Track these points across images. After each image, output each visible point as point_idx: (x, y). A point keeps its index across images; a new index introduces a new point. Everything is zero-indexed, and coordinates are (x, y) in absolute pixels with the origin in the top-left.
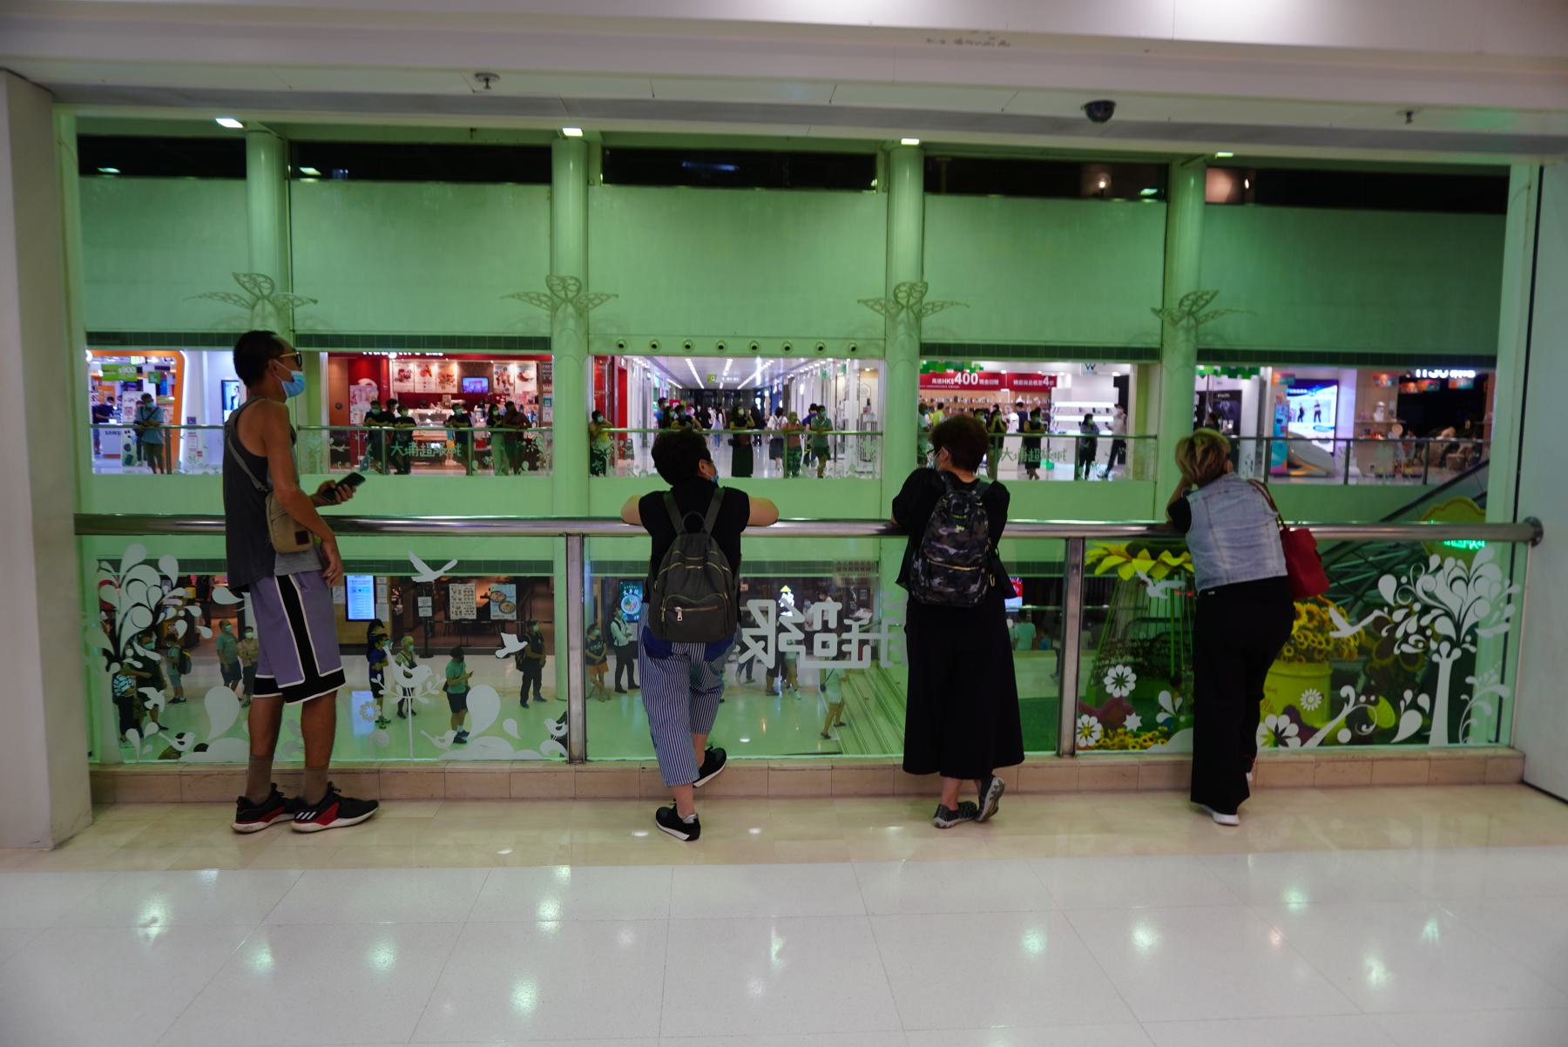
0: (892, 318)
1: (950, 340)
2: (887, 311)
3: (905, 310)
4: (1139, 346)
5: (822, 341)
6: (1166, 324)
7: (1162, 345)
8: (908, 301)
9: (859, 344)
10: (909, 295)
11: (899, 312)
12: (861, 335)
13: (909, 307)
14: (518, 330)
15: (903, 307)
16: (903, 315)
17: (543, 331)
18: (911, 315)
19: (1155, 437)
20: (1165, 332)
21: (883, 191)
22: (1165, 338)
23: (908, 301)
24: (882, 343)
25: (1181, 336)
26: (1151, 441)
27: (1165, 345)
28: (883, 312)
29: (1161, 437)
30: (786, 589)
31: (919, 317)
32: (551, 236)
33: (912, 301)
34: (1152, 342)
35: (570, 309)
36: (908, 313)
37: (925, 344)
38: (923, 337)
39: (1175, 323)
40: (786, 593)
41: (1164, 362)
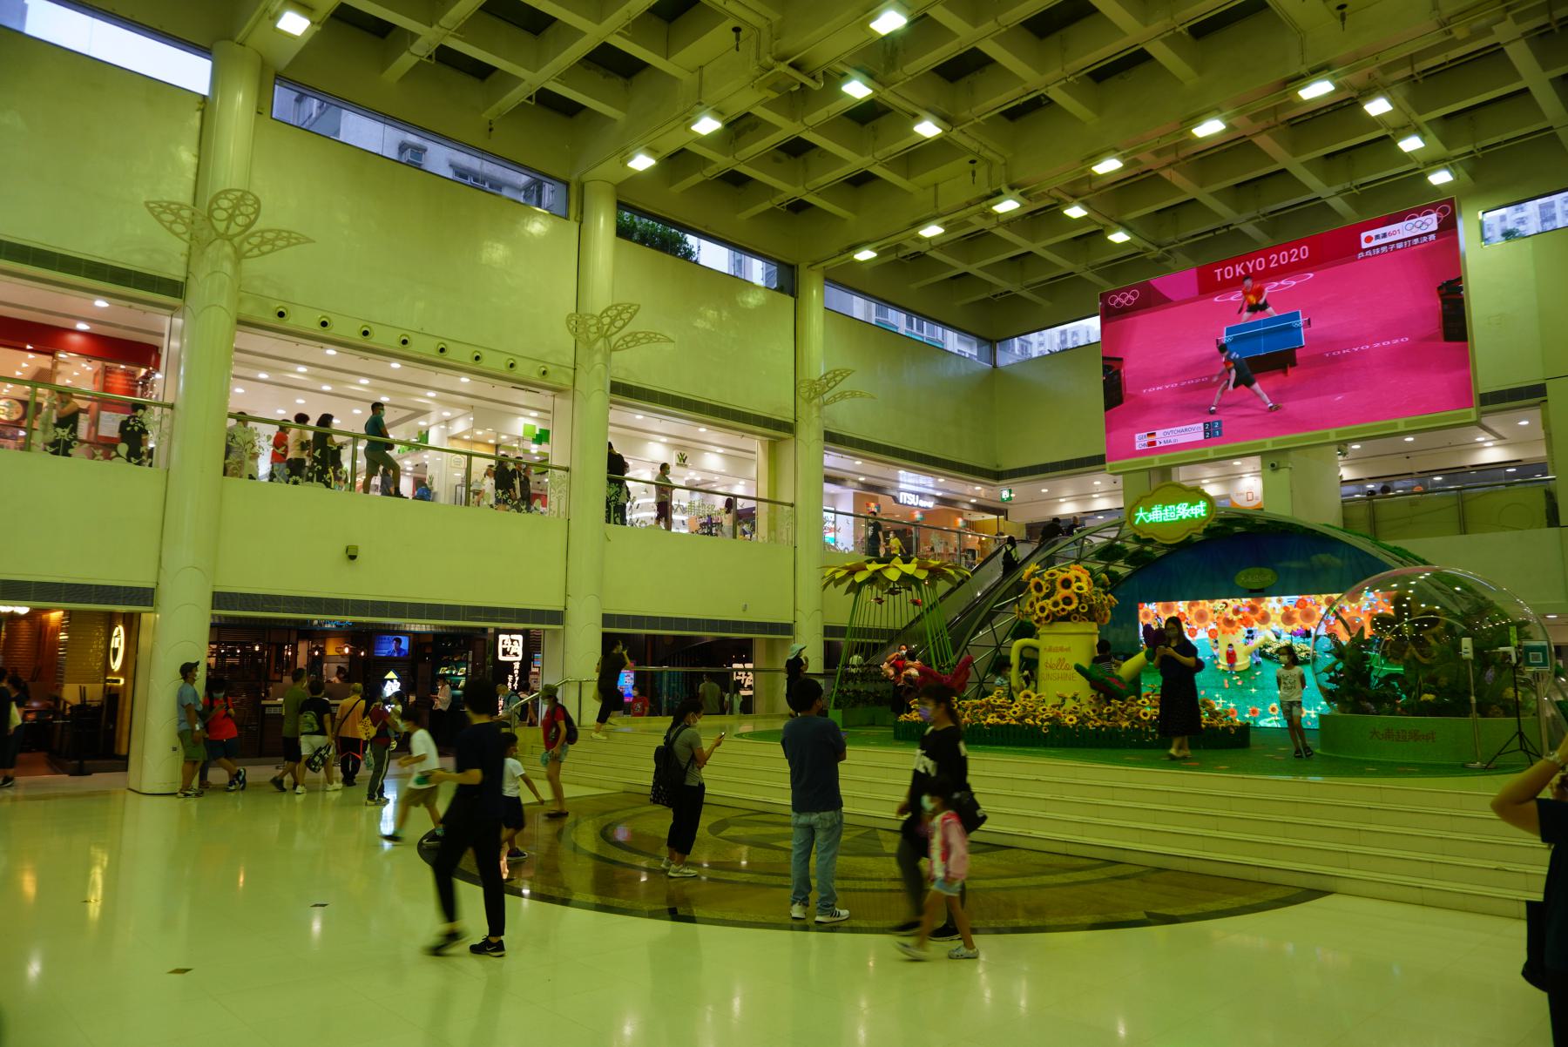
1: (632, 382)
4: (780, 418)
8: (608, 330)
9: (550, 368)
11: (596, 340)
12: (551, 359)
14: (135, 261)
16: (600, 344)
17: (175, 272)
19: (792, 505)
20: (798, 410)
23: (608, 330)
26: (787, 508)
27: (800, 420)
29: (799, 504)
30: (391, 675)
34: (788, 416)
35: (228, 249)
36: (605, 344)
40: (392, 680)
41: (799, 436)
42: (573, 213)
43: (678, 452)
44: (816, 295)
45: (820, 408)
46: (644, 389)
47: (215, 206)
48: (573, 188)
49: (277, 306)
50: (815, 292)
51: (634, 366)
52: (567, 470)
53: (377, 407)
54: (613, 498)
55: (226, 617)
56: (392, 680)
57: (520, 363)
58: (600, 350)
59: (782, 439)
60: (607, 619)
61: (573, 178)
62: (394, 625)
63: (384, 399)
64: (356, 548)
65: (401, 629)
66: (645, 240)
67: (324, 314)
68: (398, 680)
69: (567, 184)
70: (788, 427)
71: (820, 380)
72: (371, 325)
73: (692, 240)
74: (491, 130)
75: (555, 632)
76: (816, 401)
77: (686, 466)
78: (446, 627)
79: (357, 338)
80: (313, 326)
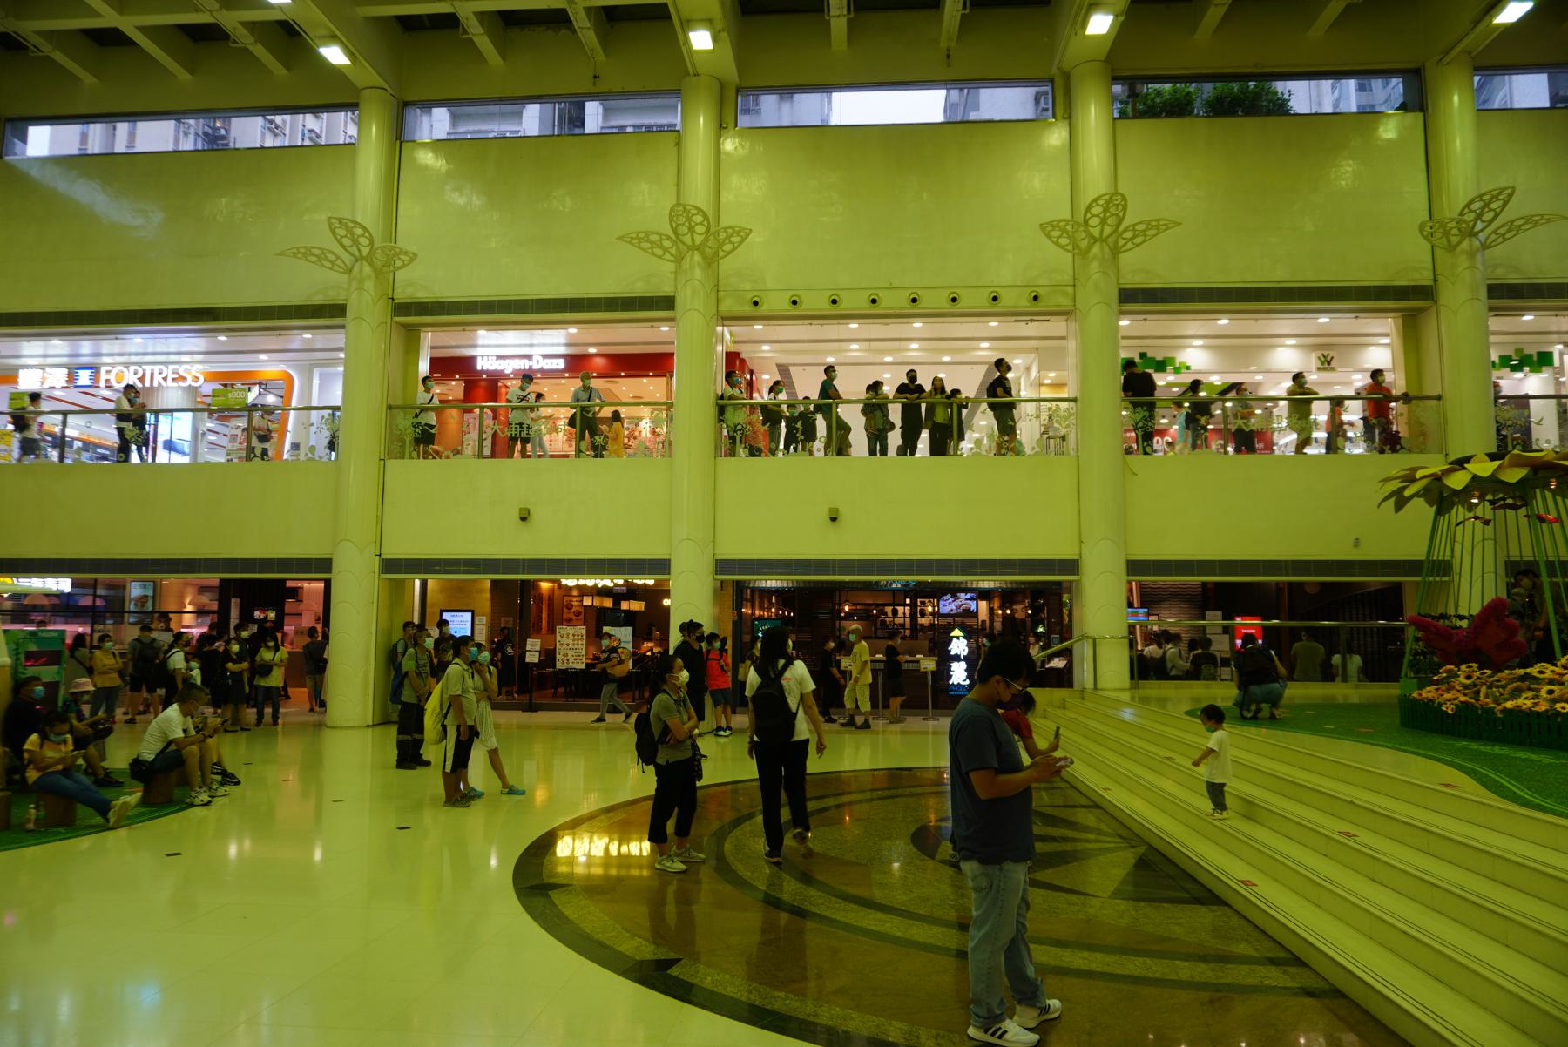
0: (1080, 254)
2: (1076, 246)
3: (1098, 244)
5: (996, 289)
6: (1439, 252)
7: (1435, 281)
8: (1102, 231)
9: (1041, 292)
10: (1103, 222)
11: (1090, 246)
12: (1043, 281)
13: (1103, 240)
14: (639, 289)
15: (1096, 241)
16: (1096, 249)
17: (666, 290)
18: (1107, 250)
19: (1439, 398)
21: (1064, 118)
22: (1439, 271)
23: (1102, 231)
24: (1070, 290)
25: (1463, 262)
27: (1440, 278)
28: (1070, 247)
29: (1447, 395)
30: (957, 632)
31: (1116, 252)
32: (678, 185)
33: (1107, 230)
34: (1423, 277)
35: (697, 257)
36: (1102, 248)
37: (1125, 289)
38: (1121, 281)
39: (1452, 248)
40: (958, 638)
42: (1059, 113)
43: (1319, 353)
44: (1456, 103)
45: (1471, 254)
46: (1174, 289)
47: (705, 223)
48: (1059, 82)
49: (749, 296)
50: (1456, 98)
51: (1141, 267)
52: (1074, 400)
53: (829, 370)
54: (1140, 425)
55: (804, 582)
56: (958, 638)
57: (1004, 294)
58: (1095, 257)
59: (1421, 310)
60: (1134, 567)
61: (1054, 71)
62: (961, 583)
63: (830, 360)
64: (837, 510)
65: (969, 586)
66: (1151, 111)
67: (952, 290)
68: (965, 637)
69: (1052, 81)
70: (1426, 293)
71: (1461, 214)
72: (956, 290)
73: (1281, 87)
74: (948, 56)
75: (1078, 581)
76: (1465, 245)
77: (1333, 369)
78: (1016, 582)
79: (827, 308)
80: (785, 307)
